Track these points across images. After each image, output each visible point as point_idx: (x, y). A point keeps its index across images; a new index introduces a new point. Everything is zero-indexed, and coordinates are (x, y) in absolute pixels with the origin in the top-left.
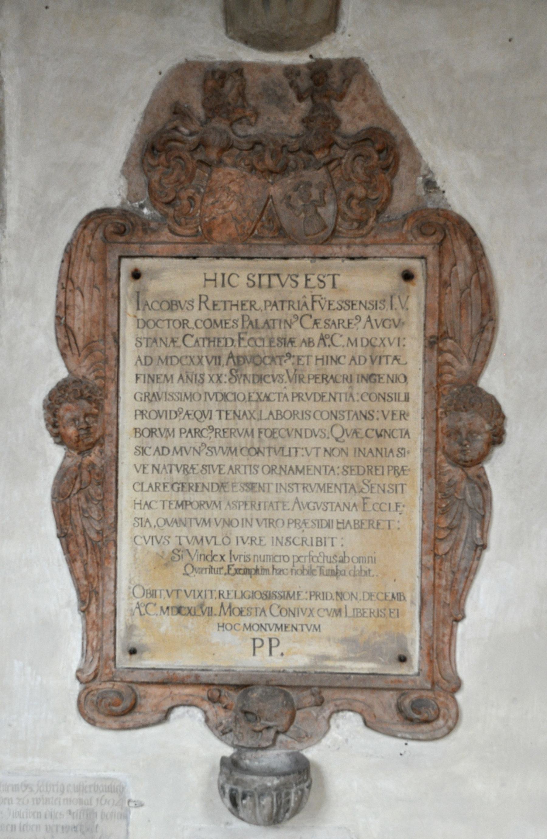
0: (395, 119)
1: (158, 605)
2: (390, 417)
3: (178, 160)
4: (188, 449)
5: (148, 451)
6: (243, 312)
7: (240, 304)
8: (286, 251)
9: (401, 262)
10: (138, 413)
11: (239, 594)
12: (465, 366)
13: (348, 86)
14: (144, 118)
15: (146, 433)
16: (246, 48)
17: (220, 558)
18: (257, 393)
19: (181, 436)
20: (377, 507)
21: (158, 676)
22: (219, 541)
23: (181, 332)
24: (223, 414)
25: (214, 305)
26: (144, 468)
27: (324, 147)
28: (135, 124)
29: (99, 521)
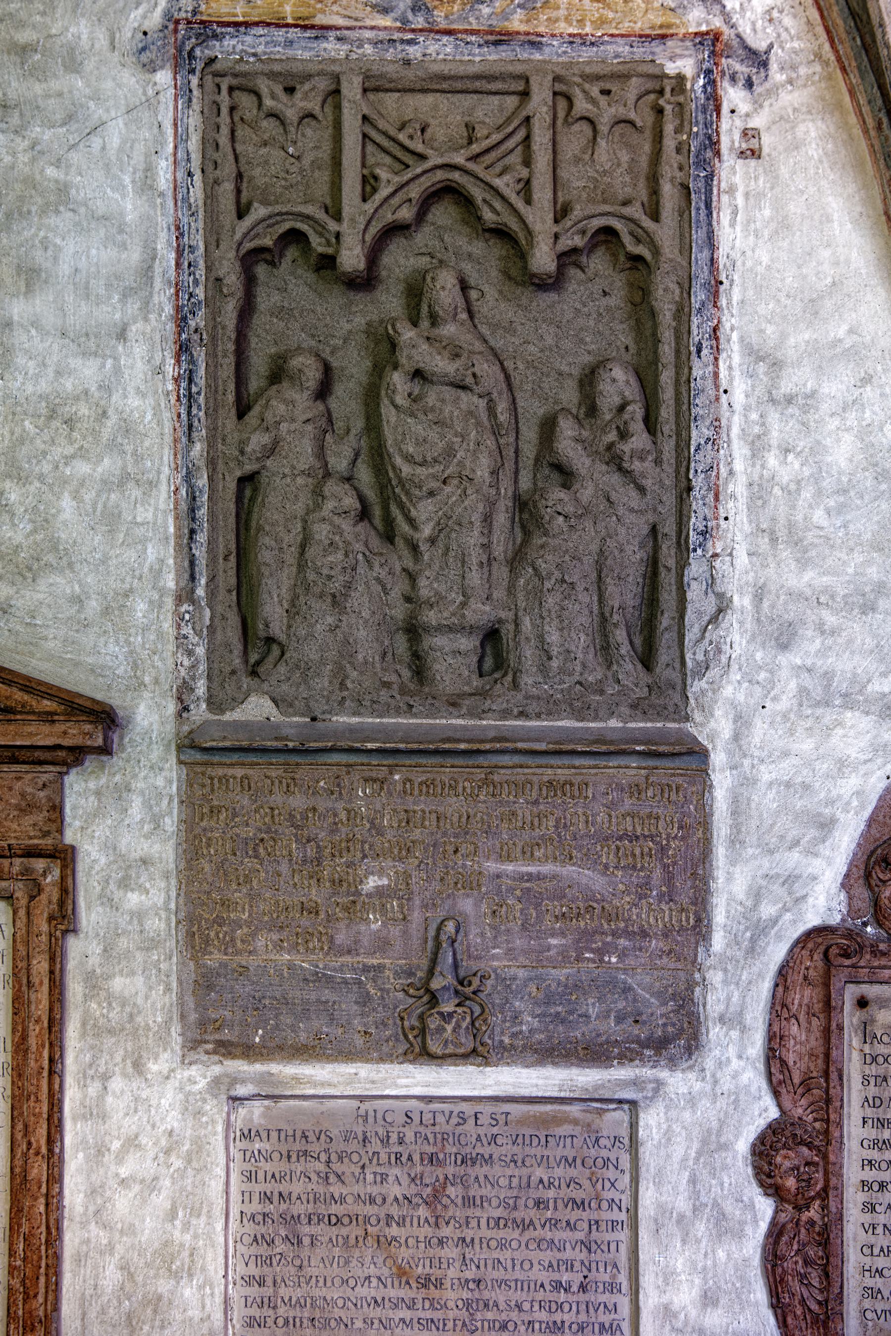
5: (877, 1207)
10: (866, 1162)
15: (876, 1187)
26: (874, 1228)
28: (859, 831)
29: (821, 1291)
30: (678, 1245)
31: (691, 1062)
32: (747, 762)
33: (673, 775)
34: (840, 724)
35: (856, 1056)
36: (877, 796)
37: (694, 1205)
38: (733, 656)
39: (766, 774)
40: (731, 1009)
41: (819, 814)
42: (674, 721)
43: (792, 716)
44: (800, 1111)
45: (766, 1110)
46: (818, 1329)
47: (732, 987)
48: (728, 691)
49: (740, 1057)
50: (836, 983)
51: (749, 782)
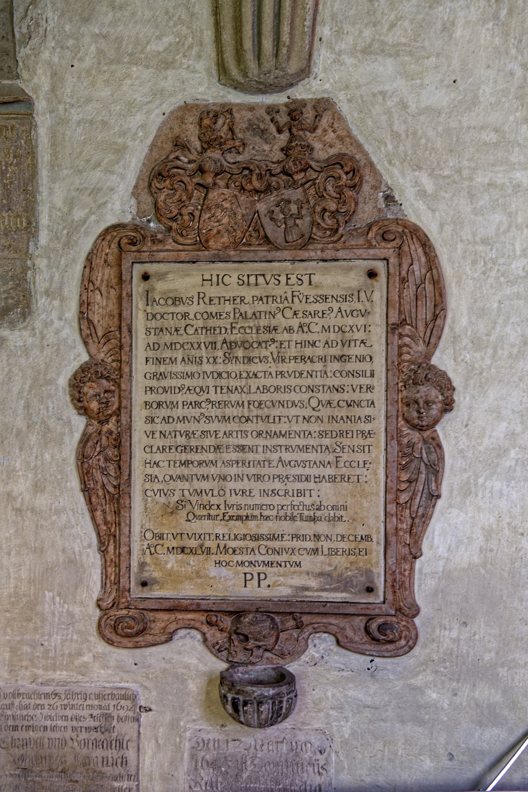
0: (359, 146)
1: (166, 546)
2: (358, 390)
3: (179, 183)
4: (189, 418)
5: (156, 420)
6: (235, 306)
7: (232, 299)
8: (270, 256)
9: (366, 262)
10: (148, 389)
11: (232, 537)
12: (421, 347)
13: (319, 121)
14: (151, 150)
15: (154, 405)
16: (234, 92)
17: (216, 507)
18: (247, 372)
19: (183, 408)
20: (347, 464)
21: (166, 605)
22: (216, 492)
23: (183, 323)
24: (219, 389)
25: (211, 300)
26: (153, 434)
27: (301, 171)
28: (144, 154)
30: (17, 451)
31: (25, 324)
32: (61, 107)
33: (8, 119)
34: (129, 76)
35: (141, 315)
36: (157, 128)
37: (28, 423)
38: (48, 29)
39: (75, 115)
40: (54, 286)
41: (115, 143)
42: (8, 78)
43: (93, 72)
44: (102, 355)
45: (79, 355)
46: (114, 504)
47: (54, 270)
48: (46, 55)
49: (60, 319)
50: (126, 265)
51: (63, 121)
